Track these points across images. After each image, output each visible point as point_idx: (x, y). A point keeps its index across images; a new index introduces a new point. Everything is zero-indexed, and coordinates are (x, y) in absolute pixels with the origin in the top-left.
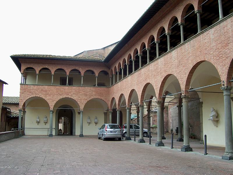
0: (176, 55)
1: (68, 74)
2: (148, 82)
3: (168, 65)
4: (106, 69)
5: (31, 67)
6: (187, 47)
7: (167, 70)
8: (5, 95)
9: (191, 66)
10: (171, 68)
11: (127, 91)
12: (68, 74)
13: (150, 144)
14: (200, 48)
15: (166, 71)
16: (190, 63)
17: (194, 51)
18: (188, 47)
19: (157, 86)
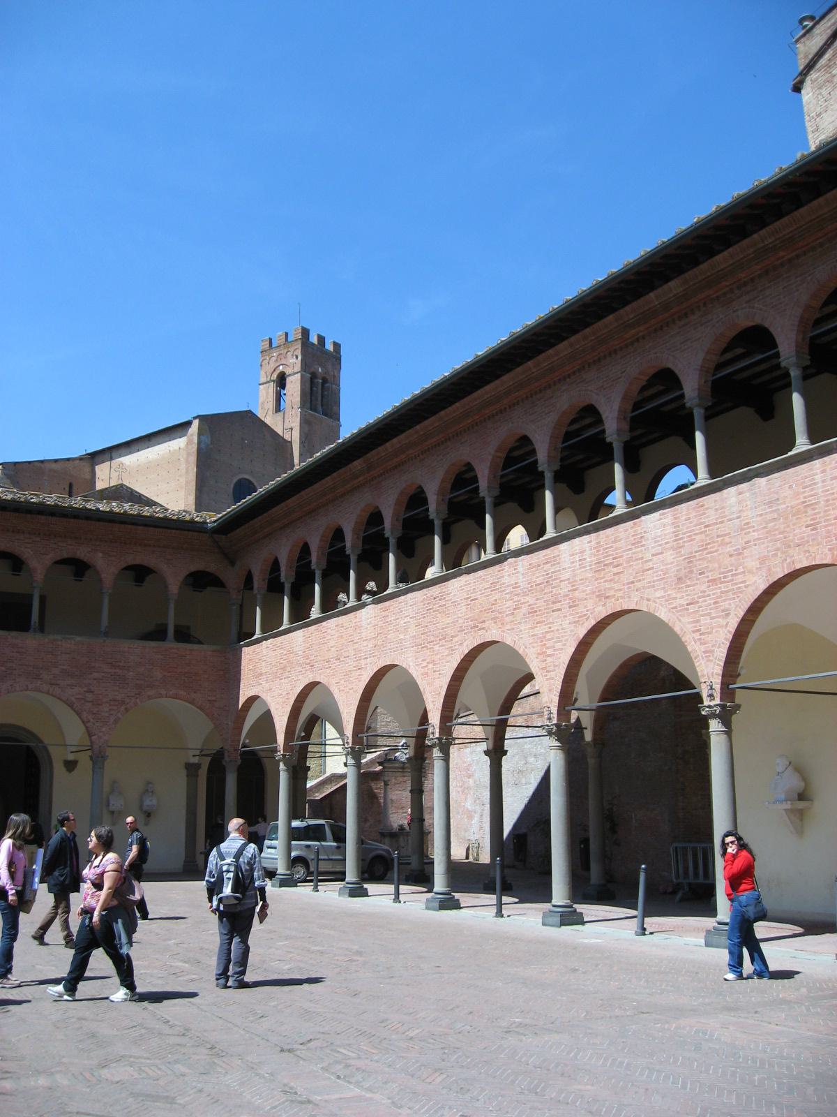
0: (670, 529)
1: (39, 576)
3: (616, 570)
4: (211, 564)
6: (733, 500)
7: (611, 593)
9: (759, 584)
10: (638, 585)
11: (348, 673)
12: (39, 576)
13: (499, 914)
14: (810, 512)
15: (607, 597)
16: (750, 572)
17: (774, 520)
18: (740, 502)
19: (549, 659)
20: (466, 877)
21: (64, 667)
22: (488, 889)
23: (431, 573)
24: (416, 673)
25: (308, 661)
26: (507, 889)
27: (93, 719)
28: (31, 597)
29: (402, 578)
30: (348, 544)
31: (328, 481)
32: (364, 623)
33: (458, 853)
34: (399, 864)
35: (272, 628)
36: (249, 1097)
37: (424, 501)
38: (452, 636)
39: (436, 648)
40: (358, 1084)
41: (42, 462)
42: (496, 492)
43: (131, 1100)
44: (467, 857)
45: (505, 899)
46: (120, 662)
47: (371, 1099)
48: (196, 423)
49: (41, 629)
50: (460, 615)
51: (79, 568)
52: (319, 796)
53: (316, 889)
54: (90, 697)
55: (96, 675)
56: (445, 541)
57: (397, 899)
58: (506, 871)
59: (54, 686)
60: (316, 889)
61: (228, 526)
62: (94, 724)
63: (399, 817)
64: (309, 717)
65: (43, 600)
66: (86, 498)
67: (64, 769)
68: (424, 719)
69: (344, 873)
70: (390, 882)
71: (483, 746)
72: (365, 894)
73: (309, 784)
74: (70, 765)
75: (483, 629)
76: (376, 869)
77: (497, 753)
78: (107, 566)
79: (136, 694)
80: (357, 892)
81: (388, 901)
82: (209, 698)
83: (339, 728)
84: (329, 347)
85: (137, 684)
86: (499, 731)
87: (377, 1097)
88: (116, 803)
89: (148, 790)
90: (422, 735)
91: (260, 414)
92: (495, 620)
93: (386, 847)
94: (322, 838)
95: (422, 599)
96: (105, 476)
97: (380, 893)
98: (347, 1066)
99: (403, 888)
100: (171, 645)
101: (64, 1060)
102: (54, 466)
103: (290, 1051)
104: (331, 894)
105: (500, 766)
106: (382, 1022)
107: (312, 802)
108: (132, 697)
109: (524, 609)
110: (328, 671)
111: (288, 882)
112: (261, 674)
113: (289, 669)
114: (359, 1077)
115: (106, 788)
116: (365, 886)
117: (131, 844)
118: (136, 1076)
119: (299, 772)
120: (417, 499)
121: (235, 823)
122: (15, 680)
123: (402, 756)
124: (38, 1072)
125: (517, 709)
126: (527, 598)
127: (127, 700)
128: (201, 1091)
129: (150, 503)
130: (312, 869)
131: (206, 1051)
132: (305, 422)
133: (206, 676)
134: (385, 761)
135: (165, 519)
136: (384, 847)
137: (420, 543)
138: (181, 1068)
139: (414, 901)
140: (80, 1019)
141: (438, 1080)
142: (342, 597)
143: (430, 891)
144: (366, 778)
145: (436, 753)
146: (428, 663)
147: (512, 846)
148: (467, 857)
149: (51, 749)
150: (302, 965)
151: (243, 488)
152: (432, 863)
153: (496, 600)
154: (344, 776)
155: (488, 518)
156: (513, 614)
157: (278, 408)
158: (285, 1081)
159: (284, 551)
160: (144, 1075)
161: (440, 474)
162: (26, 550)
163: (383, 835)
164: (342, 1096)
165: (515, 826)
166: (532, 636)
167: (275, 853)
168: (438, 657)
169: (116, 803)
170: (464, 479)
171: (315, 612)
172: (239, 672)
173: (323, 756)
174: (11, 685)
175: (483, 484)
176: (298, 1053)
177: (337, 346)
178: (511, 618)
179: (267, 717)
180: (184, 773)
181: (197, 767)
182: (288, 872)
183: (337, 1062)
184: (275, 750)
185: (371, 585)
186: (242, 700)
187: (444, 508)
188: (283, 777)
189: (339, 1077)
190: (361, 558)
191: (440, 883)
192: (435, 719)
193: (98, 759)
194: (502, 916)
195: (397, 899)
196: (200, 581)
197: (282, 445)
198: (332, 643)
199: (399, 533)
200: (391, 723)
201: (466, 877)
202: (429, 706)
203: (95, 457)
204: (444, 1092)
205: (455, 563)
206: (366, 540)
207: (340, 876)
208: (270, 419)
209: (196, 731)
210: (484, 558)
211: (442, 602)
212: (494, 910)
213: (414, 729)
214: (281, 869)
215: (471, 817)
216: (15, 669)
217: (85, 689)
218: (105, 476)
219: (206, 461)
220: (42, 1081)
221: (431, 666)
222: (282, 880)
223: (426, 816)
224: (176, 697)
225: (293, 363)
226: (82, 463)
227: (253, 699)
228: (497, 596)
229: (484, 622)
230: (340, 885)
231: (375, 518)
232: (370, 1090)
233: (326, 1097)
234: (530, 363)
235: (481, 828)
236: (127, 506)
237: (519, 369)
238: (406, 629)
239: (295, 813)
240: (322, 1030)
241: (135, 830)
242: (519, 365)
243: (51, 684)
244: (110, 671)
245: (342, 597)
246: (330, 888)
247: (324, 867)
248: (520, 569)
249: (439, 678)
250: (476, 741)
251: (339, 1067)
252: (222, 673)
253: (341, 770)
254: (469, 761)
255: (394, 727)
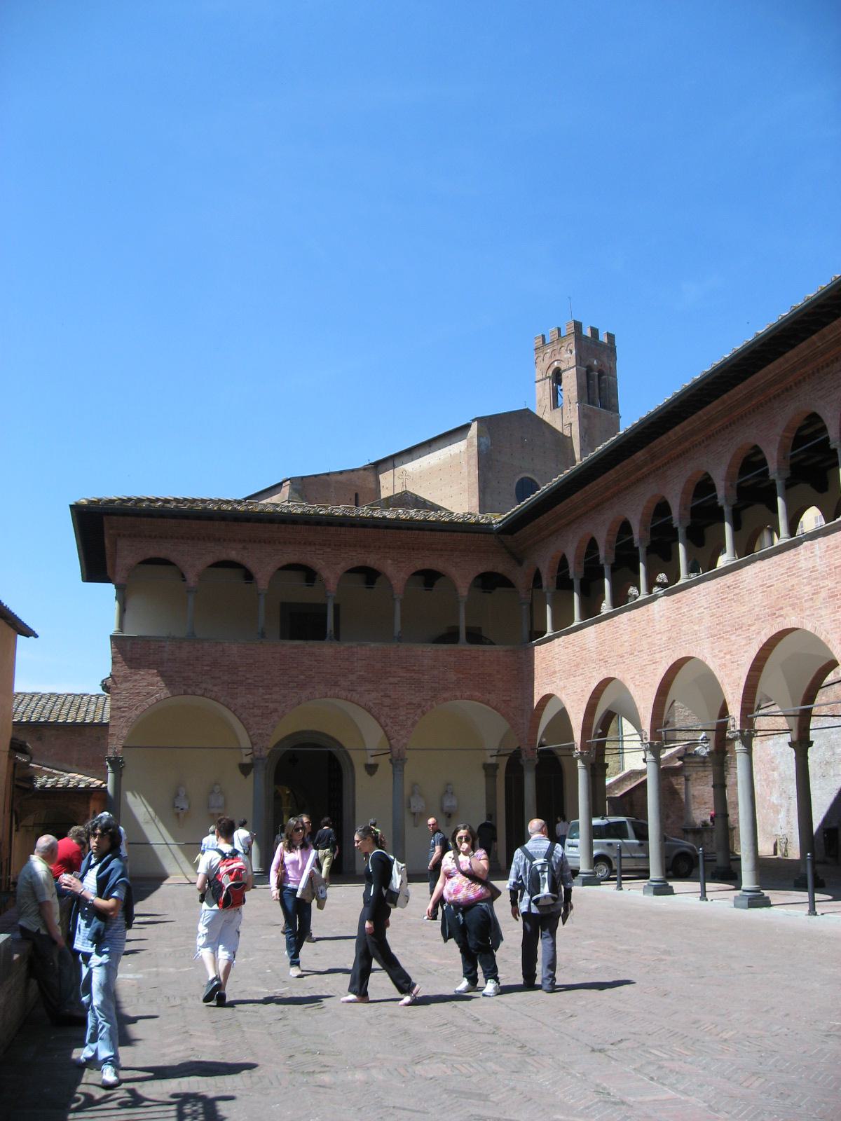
1: (332, 585)
2: (791, 621)
4: (500, 565)
5: (162, 554)
8: (23, 684)
12: (332, 585)
13: (812, 911)
20: (776, 874)
21: (361, 673)
22: (800, 885)
23: (723, 561)
24: (713, 664)
25: (601, 657)
26: (819, 886)
27: (391, 722)
28: (325, 606)
29: (692, 569)
30: (636, 537)
31: (611, 475)
32: (657, 616)
33: (765, 849)
34: (705, 861)
35: (563, 625)
36: (561, 1096)
37: (712, 488)
38: (749, 625)
39: (733, 638)
40: (672, 1086)
41: (328, 474)
42: (787, 474)
43: (445, 1096)
44: (775, 853)
45: (818, 896)
46: (415, 666)
47: (687, 1102)
48: (475, 426)
49: (337, 637)
50: (756, 603)
51: (370, 575)
52: (618, 793)
53: (620, 887)
54: (387, 701)
55: (392, 680)
56: (736, 528)
57: (703, 896)
58: (818, 867)
59: (351, 692)
60: (620, 887)
61: (512, 526)
62: (392, 728)
63: (702, 813)
64: (605, 713)
65: (337, 608)
66: (373, 507)
67: (364, 773)
68: (724, 712)
69: (648, 871)
70: (695, 879)
71: (787, 738)
72: (670, 891)
73: (609, 781)
74: (371, 769)
75: (781, 616)
76: (680, 866)
77: (802, 744)
78: (396, 572)
79: (432, 697)
80: (662, 890)
81: (694, 900)
82: (504, 698)
83: (637, 725)
84: (603, 338)
85: (432, 687)
86: (804, 719)
87: (693, 1100)
88: (417, 805)
89: (447, 791)
90: (722, 728)
91: (538, 412)
92: (793, 606)
93: (690, 844)
94: (623, 835)
95: (715, 588)
96: (390, 484)
97: (686, 892)
98: (660, 1067)
99: (709, 886)
100: (463, 647)
101: (378, 1056)
102: (340, 478)
103: (600, 1051)
104: (635, 892)
105: (806, 758)
106: (694, 1023)
107: (612, 800)
108: (429, 700)
109: (824, 594)
110: (622, 666)
111: (591, 881)
112: (555, 672)
113: (582, 666)
114: (672, 1079)
115: (407, 791)
116: (670, 884)
117: (434, 845)
118: (449, 1072)
119: (597, 770)
120: (704, 486)
121: (535, 824)
122: (314, 687)
123: (703, 750)
124: (356, 1067)
125: (821, 698)
126: (827, 582)
127: (423, 703)
128: (513, 1089)
129: (435, 508)
130: (615, 867)
131: (516, 1050)
132: (583, 416)
133: (499, 676)
134: (685, 755)
135: (451, 522)
136: (687, 844)
137: (709, 532)
138: (491, 1066)
139: (721, 899)
140: (392, 1016)
141: (757, 1084)
142: (632, 591)
143: (738, 888)
144: (666, 774)
145: (738, 746)
146: (725, 654)
147: (822, 841)
148: (775, 853)
149: (350, 752)
150: (609, 964)
151: (526, 486)
152: (739, 859)
153: (793, 586)
154: (643, 772)
155: (780, 501)
156: (812, 599)
157: (555, 405)
158: (598, 1081)
159: (571, 548)
160: (457, 1072)
161: (727, 459)
162: (317, 561)
163: (686, 831)
164: (656, 1098)
165: (825, 820)
166: (834, 620)
167: (576, 852)
168: (736, 646)
169: (417, 805)
170: (752, 462)
171: (606, 607)
172: (532, 671)
173: (621, 752)
174: (311, 693)
175: (772, 466)
176: (609, 1053)
177: (611, 337)
178: (810, 603)
179: (563, 715)
180: (482, 773)
181: (495, 767)
182: (591, 871)
183: (649, 1063)
184: (572, 748)
185: (662, 577)
186: (537, 699)
187: (734, 493)
188: (582, 775)
189: (652, 1079)
190: (649, 551)
191: (748, 879)
192: (735, 711)
193: (398, 762)
194: (816, 914)
195: (703, 896)
196: (488, 582)
197: (562, 442)
198: (625, 638)
199: (688, 522)
200: (689, 718)
201: (776, 874)
202: (729, 698)
203: (379, 466)
204: (763, 1096)
205: (747, 549)
206: (654, 531)
207: (644, 874)
208: (549, 416)
209: (493, 732)
210: (777, 542)
211: (737, 591)
212: (806, 908)
213: (714, 722)
214: (584, 867)
215: (777, 812)
216: (314, 677)
217: (382, 694)
218: (390, 484)
219: (487, 463)
220: (359, 1076)
221: (728, 657)
222: (584, 879)
223: (730, 812)
224: (471, 698)
225: (567, 358)
226: (366, 473)
227: (547, 698)
228: (794, 581)
229: (781, 608)
230: (642, 883)
231: (662, 509)
232: (685, 1092)
233: (640, 1099)
234: (814, 337)
235: (788, 822)
236: (412, 512)
237: (803, 345)
238: (700, 620)
239: (595, 811)
240: (633, 1030)
241: (436, 831)
242: (804, 339)
243: (349, 690)
244: (405, 675)
245: (632, 591)
246: (634, 886)
247: (627, 864)
248: (817, 552)
249: (737, 669)
250: (779, 732)
251: (652, 1068)
252: (515, 672)
253: (640, 766)
254: (772, 754)
255: (692, 721)
